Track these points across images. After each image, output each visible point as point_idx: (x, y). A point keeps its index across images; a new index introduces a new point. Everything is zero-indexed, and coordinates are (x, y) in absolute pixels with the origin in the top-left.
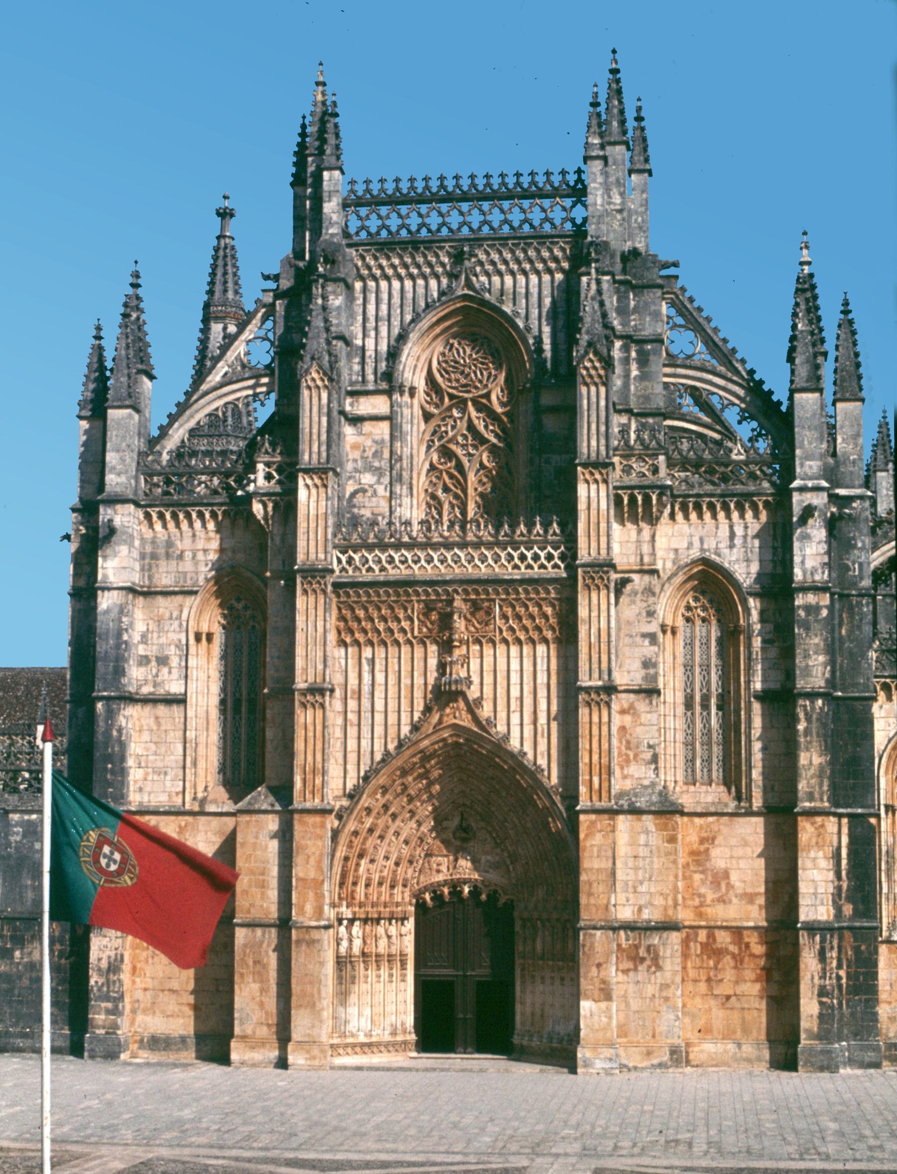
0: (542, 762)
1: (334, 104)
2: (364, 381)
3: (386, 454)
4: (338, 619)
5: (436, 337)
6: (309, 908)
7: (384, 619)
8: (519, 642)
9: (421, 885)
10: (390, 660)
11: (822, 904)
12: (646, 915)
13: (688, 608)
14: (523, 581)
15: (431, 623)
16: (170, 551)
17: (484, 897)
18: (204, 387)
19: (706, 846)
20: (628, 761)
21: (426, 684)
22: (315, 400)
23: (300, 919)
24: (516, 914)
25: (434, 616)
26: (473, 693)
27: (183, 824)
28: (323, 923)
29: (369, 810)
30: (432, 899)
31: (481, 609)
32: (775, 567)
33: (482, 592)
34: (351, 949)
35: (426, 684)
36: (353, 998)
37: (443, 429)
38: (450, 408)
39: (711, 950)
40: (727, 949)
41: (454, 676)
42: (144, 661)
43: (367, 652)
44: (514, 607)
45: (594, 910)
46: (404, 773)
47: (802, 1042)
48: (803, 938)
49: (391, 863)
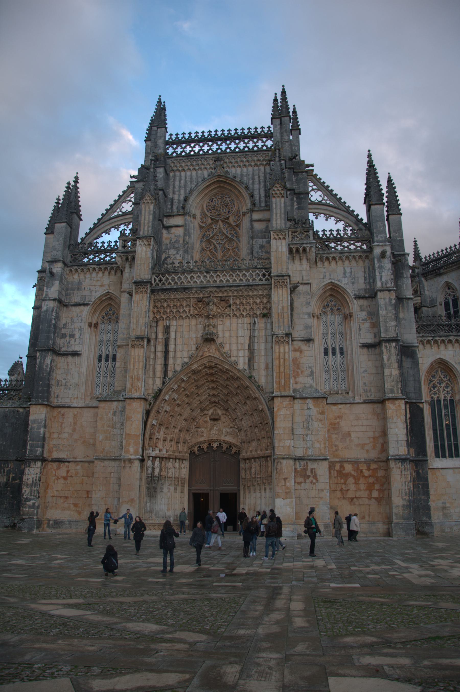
0: (255, 374)
1: (164, 106)
2: (172, 212)
3: (181, 241)
4: (154, 308)
5: (205, 195)
6: (132, 450)
11: (401, 446)
12: (310, 452)
13: (324, 307)
16: (79, 286)
18: (102, 221)
19: (338, 420)
20: (298, 375)
22: (147, 209)
25: (200, 305)
26: (219, 341)
27: (76, 413)
28: (138, 457)
32: (366, 286)
37: (208, 233)
38: (211, 224)
39: (342, 474)
40: (351, 473)
42: (63, 336)
45: (282, 448)
47: (394, 521)
48: (392, 464)
49: (176, 431)
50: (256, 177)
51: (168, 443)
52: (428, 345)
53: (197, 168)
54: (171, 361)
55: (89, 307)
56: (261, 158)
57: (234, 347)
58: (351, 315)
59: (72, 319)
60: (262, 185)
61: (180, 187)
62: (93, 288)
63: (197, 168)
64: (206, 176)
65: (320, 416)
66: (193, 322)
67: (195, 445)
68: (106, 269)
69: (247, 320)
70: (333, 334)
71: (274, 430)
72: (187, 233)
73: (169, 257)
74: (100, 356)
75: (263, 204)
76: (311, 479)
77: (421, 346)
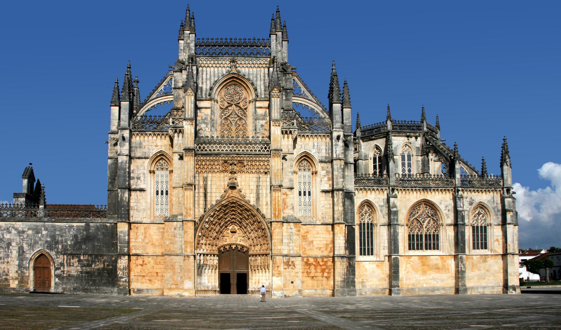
2: (202, 97)
3: (209, 119)
12: (291, 252)
16: (140, 146)
20: (285, 208)
25: (226, 164)
38: (227, 107)
43: (205, 175)
50: (258, 76)
51: (208, 246)
52: (361, 191)
53: (218, 65)
54: (209, 199)
55: (148, 160)
56: (262, 62)
57: (248, 191)
58: (316, 173)
59: (137, 167)
60: (262, 82)
61: (206, 79)
62: (150, 147)
63: (218, 65)
64: (224, 73)
65: (297, 233)
66: (222, 175)
68: (159, 134)
69: (256, 175)
70: (305, 183)
71: (271, 240)
72: (212, 113)
73: (201, 129)
74: (157, 192)
75: (263, 96)
76: (292, 266)
77: (356, 192)
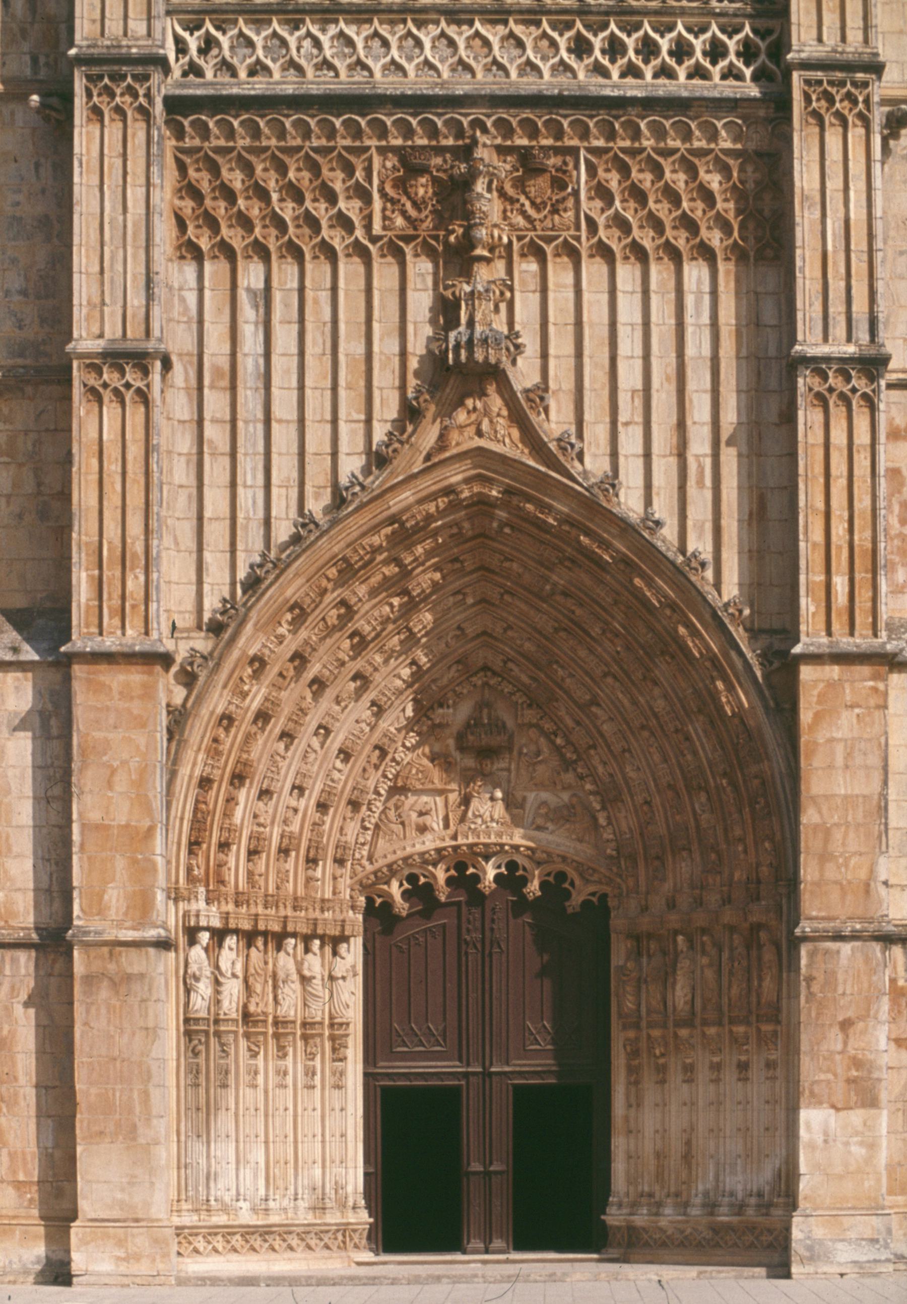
7: (295, 194)
8: (639, 253)
9: (381, 863)
10: (309, 294)
14: (649, 104)
15: (415, 204)
17: (534, 888)
21: (403, 354)
23: (95, 924)
24: (617, 922)
25: (422, 188)
26: (524, 374)
28: (152, 933)
29: (259, 663)
30: (406, 895)
31: (541, 171)
33: (545, 131)
34: (218, 1002)
35: (403, 354)
36: (224, 1122)
41: (478, 329)
44: (624, 170)
46: (348, 571)
67: (393, 870)
